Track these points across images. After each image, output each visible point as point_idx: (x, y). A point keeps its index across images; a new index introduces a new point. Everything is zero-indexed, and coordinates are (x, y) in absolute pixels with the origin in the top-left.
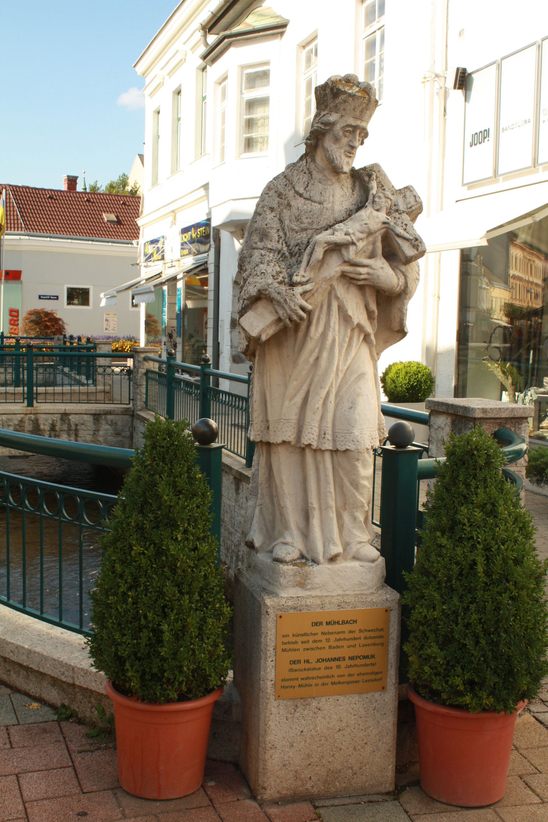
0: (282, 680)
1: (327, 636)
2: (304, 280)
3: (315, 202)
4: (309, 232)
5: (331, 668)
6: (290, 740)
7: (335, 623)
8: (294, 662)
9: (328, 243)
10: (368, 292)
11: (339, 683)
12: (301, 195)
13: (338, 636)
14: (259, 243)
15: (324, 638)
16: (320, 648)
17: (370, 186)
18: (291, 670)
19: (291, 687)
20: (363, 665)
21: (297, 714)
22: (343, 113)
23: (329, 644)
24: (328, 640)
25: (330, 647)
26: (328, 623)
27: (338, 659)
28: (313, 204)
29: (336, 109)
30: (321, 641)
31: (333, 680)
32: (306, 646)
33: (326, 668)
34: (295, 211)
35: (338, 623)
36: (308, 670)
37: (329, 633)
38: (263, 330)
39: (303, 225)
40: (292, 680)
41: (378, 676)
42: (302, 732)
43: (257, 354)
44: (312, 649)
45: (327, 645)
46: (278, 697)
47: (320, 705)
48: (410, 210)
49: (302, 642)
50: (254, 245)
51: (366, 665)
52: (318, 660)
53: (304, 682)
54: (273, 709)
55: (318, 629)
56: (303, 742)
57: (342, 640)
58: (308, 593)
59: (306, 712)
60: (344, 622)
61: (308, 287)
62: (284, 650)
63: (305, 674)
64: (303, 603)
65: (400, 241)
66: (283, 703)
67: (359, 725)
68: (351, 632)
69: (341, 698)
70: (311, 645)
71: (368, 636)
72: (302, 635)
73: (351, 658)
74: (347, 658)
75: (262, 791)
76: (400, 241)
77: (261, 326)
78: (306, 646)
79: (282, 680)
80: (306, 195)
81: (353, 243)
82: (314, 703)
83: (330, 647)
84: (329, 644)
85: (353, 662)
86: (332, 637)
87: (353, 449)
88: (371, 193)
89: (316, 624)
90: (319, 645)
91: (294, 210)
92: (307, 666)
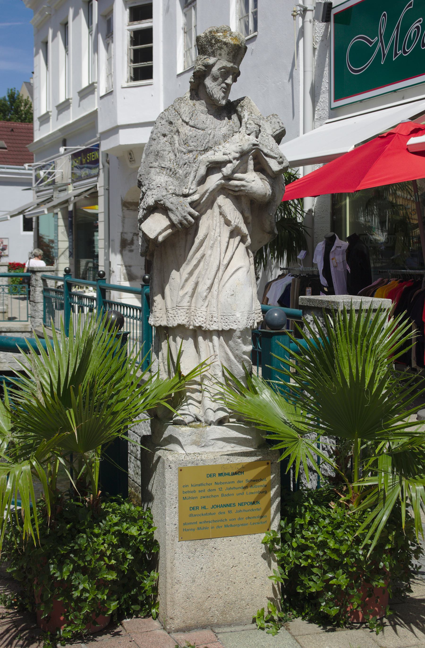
0: (184, 524)
1: (220, 486)
2: (191, 191)
3: (198, 129)
4: (194, 153)
5: (224, 513)
6: (192, 576)
8: (193, 508)
9: (211, 163)
11: (231, 526)
12: (187, 123)
13: (229, 486)
14: (155, 163)
15: (217, 487)
16: (214, 496)
17: (242, 115)
18: (191, 515)
19: (192, 529)
20: (250, 510)
21: (197, 554)
22: (220, 58)
24: (220, 489)
25: (222, 495)
26: (220, 475)
27: (230, 505)
28: (197, 130)
29: (213, 54)
32: (203, 494)
33: (220, 513)
34: (183, 136)
35: (228, 474)
38: (160, 233)
39: (189, 148)
40: (192, 523)
42: (202, 569)
43: (155, 254)
44: (208, 497)
46: (181, 539)
47: (216, 546)
48: (275, 134)
49: (199, 491)
50: (151, 165)
52: (213, 507)
54: (177, 549)
55: (212, 480)
57: (232, 489)
58: (203, 450)
59: (205, 551)
61: (196, 197)
62: (184, 498)
64: (199, 458)
65: (267, 159)
66: (185, 543)
67: (249, 562)
69: (233, 539)
70: (207, 493)
73: (241, 504)
74: (237, 504)
75: (170, 621)
76: (267, 159)
77: (159, 230)
78: (203, 494)
79: (184, 524)
80: (191, 123)
81: (230, 162)
83: (222, 495)
85: (242, 508)
86: (224, 486)
87: (235, 329)
88: (243, 120)
89: (210, 476)
90: (213, 493)
91: (182, 136)
92: (204, 511)
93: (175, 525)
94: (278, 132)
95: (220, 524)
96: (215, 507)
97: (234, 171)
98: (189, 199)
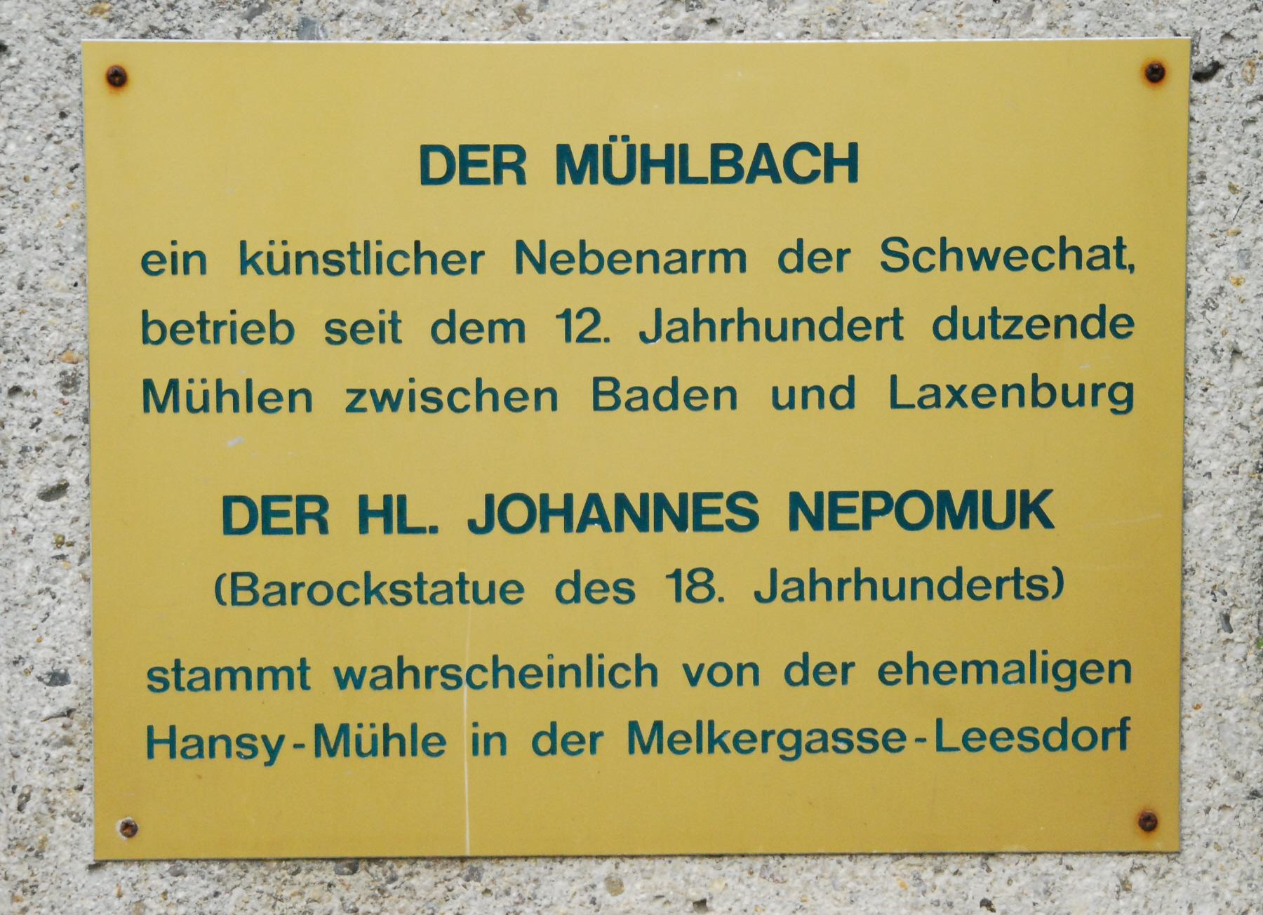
0: (158, 680)
1: (576, 290)
7: (642, 163)
8: (264, 514)
15: (541, 297)
18: (238, 588)
24: (582, 326)
25: (604, 392)
26: (578, 165)
27: (690, 513)
32: (378, 366)
33: (576, 589)
40: (253, 678)
44: (432, 400)
49: (336, 332)
51: (962, 586)
52: (494, 513)
60: (727, 164)
62: (159, 397)
68: (802, 258)
73: (818, 512)
74: (773, 510)
78: (378, 366)
83: (604, 392)
85: (831, 552)
86: (627, 301)
89: (462, 165)
92: (390, 557)
93: (58, 678)
95: (576, 707)
96: (517, 513)
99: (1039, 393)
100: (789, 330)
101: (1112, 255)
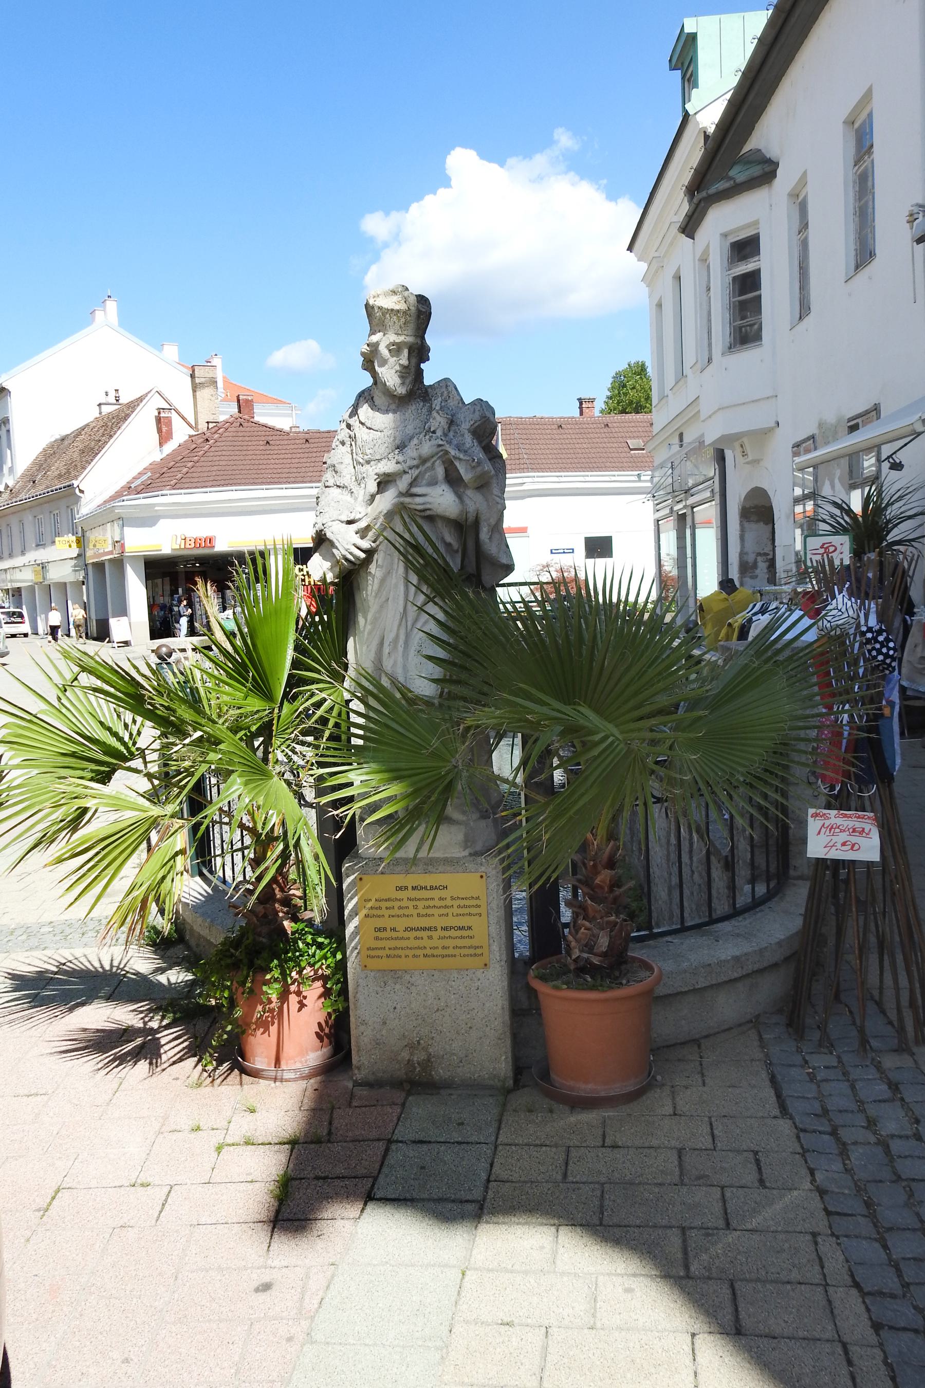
0: (368, 949)
1: (415, 903)
7: (422, 888)
8: (379, 930)
10: (440, 524)
16: (408, 916)
18: (377, 938)
19: (378, 957)
23: (417, 911)
24: (416, 907)
25: (418, 915)
26: (414, 888)
27: (430, 929)
30: (407, 907)
31: (425, 952)
32: (392, 912)
33: (416, 938)
35: (426, 888)
36: (396, 939)
37: (416, 899)
41: (478, 951)
42: (395, 1008)
45: (415, 912)
49: (387, 908)
51: (462, 937)
52: (406, 929)
53: (392, 952)
56: (397, 1020)
59: (398, 987)
60: (432, 888)
63: (393, 944)
65: (457, 464)
68: (441, 899)
70: (396, 911)
71: (462, 905)
72: (386, 900)
73: (445, 929)
78: (392, 912)
79: (368, 949)
82: (407, 977)
83: (418, 915)
84: (417, 911)
85: (447, 934)
86: (421, 904)
89: (401, 888)
92: (394, 935)
94: (478, 423)
95: (418, 952)
97: (411, 485)
98: (355, 527)
99: (470, 914)
100: (440, 907)
101: (478, 898)
